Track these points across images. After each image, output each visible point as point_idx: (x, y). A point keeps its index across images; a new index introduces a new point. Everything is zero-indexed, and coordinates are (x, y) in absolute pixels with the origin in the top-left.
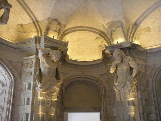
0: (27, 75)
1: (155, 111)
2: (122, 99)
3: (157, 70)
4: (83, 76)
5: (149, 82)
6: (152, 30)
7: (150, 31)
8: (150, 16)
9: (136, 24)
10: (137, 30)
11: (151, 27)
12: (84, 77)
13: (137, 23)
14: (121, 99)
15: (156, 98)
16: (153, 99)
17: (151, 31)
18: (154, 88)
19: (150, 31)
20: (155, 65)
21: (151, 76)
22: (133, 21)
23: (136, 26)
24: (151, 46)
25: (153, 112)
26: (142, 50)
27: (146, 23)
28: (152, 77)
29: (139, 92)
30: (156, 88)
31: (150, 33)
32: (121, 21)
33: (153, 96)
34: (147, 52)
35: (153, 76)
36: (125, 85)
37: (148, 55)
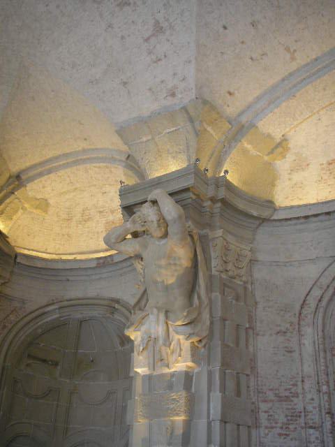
3: (24, 314)
6: (51, 210)
7: (46, 211)
8: (60, 174)
9: (18, 177)
10: (16, 193)
11: (51, 202)
13: (24, 177)
17: (49, 213)
19: (46, 211)
20: (23, 302)
22: (15, 168)
23: (17, 183)
24: (35, 248)
26: (6, 250)
27: (44, 187)
31: (43, 214)
34: (18, 260)
35: (10, 326)
37: (16, 270)
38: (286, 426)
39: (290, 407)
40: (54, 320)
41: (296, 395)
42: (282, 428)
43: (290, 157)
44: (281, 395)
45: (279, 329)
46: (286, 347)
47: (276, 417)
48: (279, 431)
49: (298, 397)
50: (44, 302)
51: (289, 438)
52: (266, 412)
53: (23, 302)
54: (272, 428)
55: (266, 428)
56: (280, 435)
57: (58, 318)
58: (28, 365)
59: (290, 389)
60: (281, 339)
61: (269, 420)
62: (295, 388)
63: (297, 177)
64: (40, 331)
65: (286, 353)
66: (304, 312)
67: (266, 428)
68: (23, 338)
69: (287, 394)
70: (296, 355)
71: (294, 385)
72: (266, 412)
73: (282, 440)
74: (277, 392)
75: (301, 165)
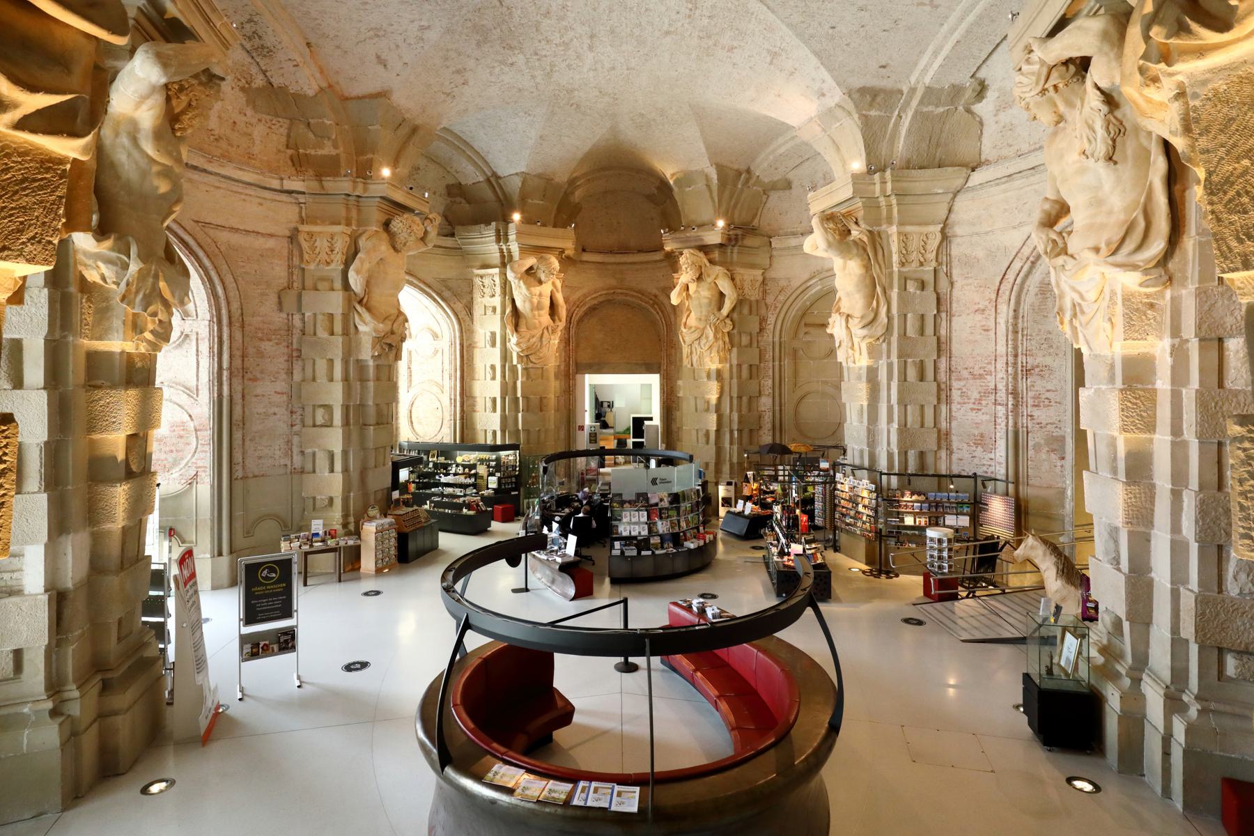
0: (485, 314)
1: (771, 391)
2: (694, 364)
3: (791, 291)
4: (620, 291)
5: (768, 322)
12: (622, 293)
14: (692, 365)
15: (777, 363)
16: (771, 363)
18: (777, 339)
20: (789, 280)
21: (776, 307)
25: (767, 393)
28: (778, 310)
29: (735, 350)
30: (780, 337)
32: (706, 171)
33: (771, 358)
36: (702, 335)
38: (979, 401)
39: (984, 384)
40: (818, 291)
41: (990, 373)
42: (974, 403)
43: (991, 95)
44: (975, 373)
45: (976, 307)
46: (984, 326)
47: (969, 393)
48: (972, 406)
49: (991, 375)
50: (806, 276)
51: (980, 413)
52: (959, 389)
53: (789, 280)
54: (964, 403)
55: (959, 403)
56: (972, 409)
57: (821, 289)
58: (806, 333)
59: (985, 367)
60: (978, 317)
61: (961, 396)
62: (989, 366)
63: (1004, 117)
64: (808, 303)
65: (983, 332)
66: (1002, 287)
67: (959, 403)
68: (793, 313)
69: (982, 372)
70: (992, 333)
71: (988, 364)
72: (959, 389)
73: (974, 413)
74: (972, 370)
75: (1005, 104)
